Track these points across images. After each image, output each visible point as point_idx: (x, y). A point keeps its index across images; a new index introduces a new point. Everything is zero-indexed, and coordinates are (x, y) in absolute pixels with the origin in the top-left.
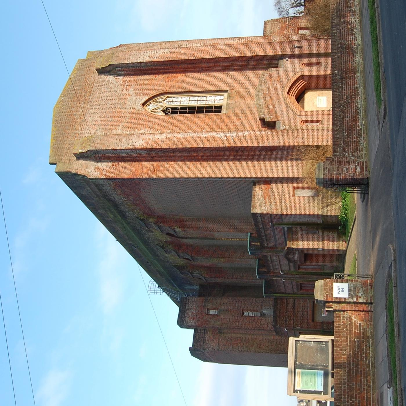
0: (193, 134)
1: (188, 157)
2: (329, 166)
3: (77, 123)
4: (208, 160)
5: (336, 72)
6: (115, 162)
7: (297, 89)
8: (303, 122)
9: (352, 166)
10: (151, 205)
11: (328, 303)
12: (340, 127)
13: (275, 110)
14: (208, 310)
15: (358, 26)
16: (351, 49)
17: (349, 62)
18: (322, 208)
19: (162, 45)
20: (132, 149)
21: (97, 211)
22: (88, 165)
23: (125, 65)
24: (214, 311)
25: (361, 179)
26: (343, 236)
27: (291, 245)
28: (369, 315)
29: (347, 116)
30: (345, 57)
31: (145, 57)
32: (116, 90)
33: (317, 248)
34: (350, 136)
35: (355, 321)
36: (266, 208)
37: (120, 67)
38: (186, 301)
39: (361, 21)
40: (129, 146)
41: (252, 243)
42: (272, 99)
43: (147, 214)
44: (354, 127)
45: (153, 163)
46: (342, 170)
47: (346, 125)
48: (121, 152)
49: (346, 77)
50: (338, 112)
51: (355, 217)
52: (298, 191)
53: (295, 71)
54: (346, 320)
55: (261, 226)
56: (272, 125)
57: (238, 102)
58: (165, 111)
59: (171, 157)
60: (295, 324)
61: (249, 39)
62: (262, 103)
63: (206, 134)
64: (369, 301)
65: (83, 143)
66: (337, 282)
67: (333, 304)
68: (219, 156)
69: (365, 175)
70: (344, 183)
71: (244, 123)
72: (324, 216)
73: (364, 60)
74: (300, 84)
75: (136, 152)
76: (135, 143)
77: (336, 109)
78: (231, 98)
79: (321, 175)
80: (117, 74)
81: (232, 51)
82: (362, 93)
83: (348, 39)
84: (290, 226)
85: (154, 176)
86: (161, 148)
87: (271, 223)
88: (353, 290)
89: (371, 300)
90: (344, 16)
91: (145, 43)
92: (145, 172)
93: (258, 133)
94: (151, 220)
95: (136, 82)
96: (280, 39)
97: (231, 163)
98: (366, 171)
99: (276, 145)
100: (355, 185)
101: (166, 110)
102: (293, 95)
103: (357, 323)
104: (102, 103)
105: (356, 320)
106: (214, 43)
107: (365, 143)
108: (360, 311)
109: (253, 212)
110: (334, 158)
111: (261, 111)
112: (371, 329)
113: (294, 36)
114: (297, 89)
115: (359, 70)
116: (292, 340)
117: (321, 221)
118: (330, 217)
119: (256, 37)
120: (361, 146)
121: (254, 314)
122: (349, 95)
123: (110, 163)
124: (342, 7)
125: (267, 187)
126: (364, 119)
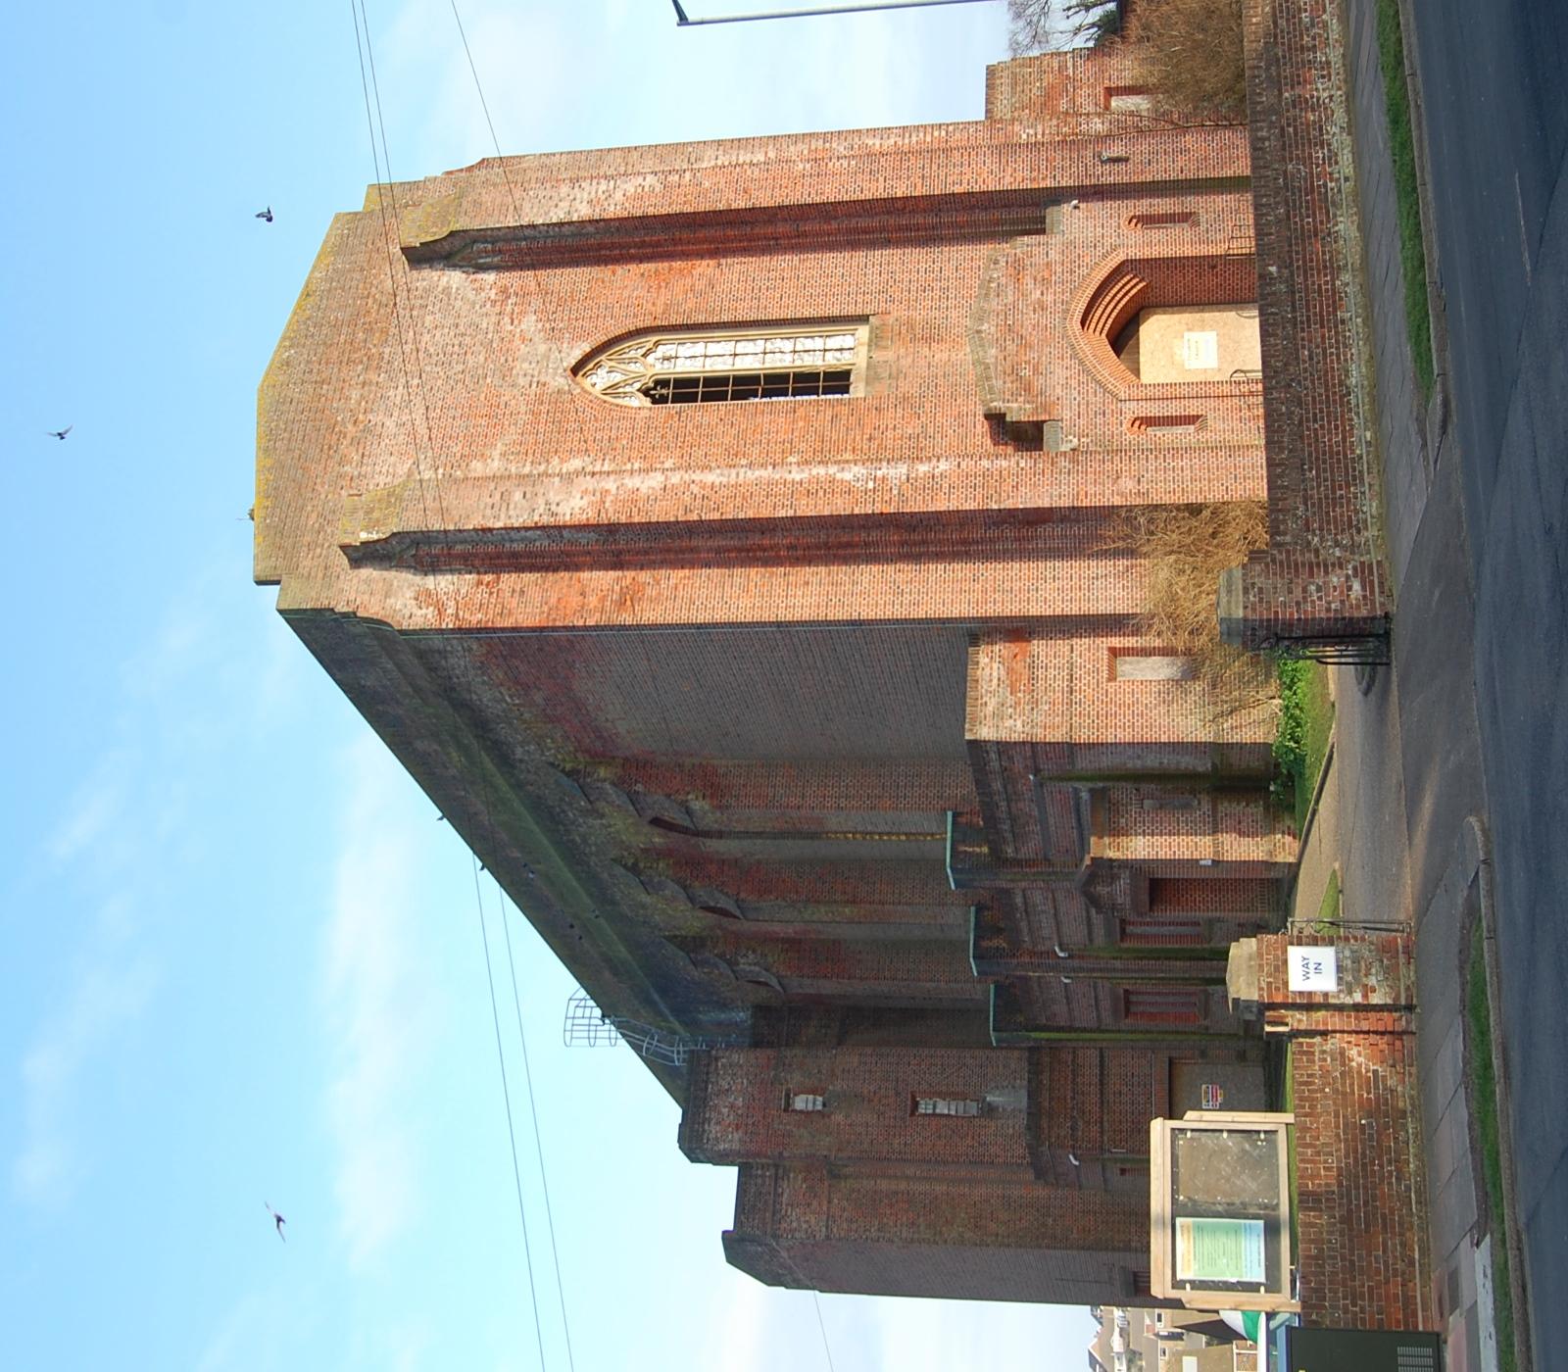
0: (757, 473)
1: (739, 550)
2: (1263, 579)
3: (345, 437)
4: (809, 561)
5: (1273, 269)
6: (486, 573)
7: (1115, 308)
8: (1137, 423)
9: (1335, 579)
10: (607, 720)
11: (1274, 1009)
12: (1290, 451)
13: (1038, 383)
14: (788, 1096)
15: (1340, 115)
16: (1320, 193)
17: (1316, 235)
18: (1211, 718)
19: (631, 161)
20: (548, 526)
21: (410, 743)
22: (392, 585)
23: (506, 234)
24: (811, 1097)
25: (1365, 619)
26: (1287, 817)
27: (1105, 849)
28: (1403, 1046)
29: (1315, 414)
30: (1302, 220)
31: (576, 204)
32: (477, 320)
33: (1197, 861)
34: (1326, 480)
35: (1360, 1065)
36: (1019, 723)
37: (486, 242)
38: (709, 1065)
39: (1350, 98)
40: (536, 518)
41: (962, 848)
42: (1029, 346)
43: (587, 751)
44: (1338, 453)
45: (620, 573)
46: (1305, 590)
47: (1310, 445)
48: (506, 537)
49: (1307, 286)
51: (1333, 747)
52: (1126, 662)
55: (997, 786)
56: (1030, 437)
57: (907, 355)
58: (652, 392)
59: (682, 551)
60: (1106, 1138)
61: (936, 134)
62: (993, 360)
63: (803, 470)
64: (1403, 1002)
65: (372, 510)
67: (1290, 1013)
68: (849, 545)
69: (1377, 605)
70: (1309, 633)
71: (931, 431)
72: (1218, 748)
73: (1364, 228)
74: (1124, 291)
75: (562, 536)
76: (558, 504)
77: (1275, 395)
78: (883, 343)
79: (1237, 608)
80: (477, 264)
81: (881, 179)
82: (1359, 340)
83: (1308, 160)
84: (1101, 785)
85: (626, 618)
86: (650, 523)
87: (1035, 776)
88: (1349, 966)
89: (1409, 997)
90: (1292, 80)
91: (570, 153)
92: (592, 606)
93: (985, 463)
94: (602, 772)
96: (1047, 132)
97: (890, 568)
99: (1047, 505)
100: (1347, 640)
101: (655, 388)
102: (1099, 329)
103: (1367, 1071)
104: (428, 369)
105: (1361, 1059)
106: (813, 147)
107: (1374, 504)
108: (1376, 1032)
109: (972, 738)
110: (1275, 552)
111: (991, 388)
112: (1412, 1089)
113: (1096, 120)
114: (1115, 308)
116: (1159, 1130)
117: (1209, 765)
118: (1241, 748)
119: (961, 127)
120: (1363, 513)
121: (953, 1107)
123: (467, 576)
124: (1284, 51)
125: (1017, 650)
126: (1369, 424)
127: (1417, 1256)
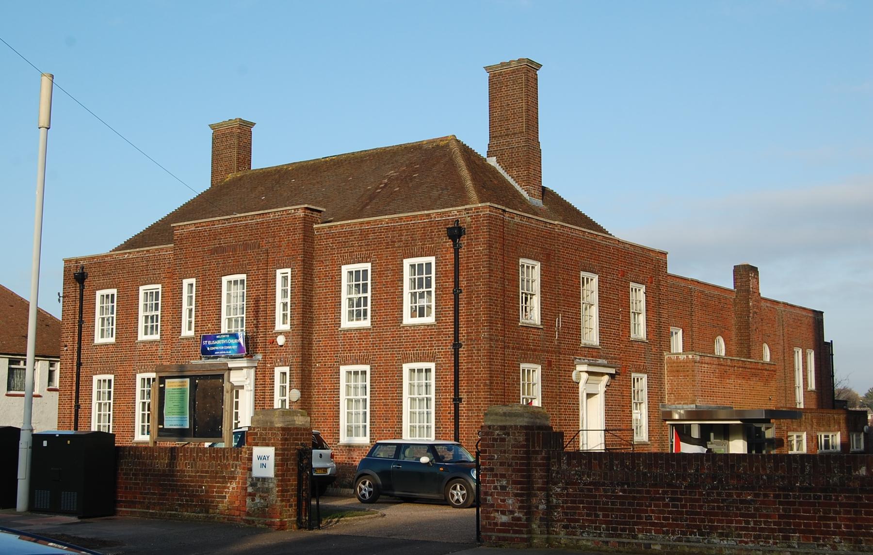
5: (863, 471)
12: (645, 474)
29: (680, 500)
34: (613, 503)
35: (228, 488)
44: (640, 517)
46: (503, 476)
47: (648, 492)
50: (697, 470)
54: (232, 471)
66: (276, 455)
69: (489, 534)
77: (706, 464)
98: (499, 538)
103: (226, 492)
107: (589, 544)
115: (863, 551)
120: (582, 533)
122: (756, 509)
126: (669, 549)
127: (151, 511)
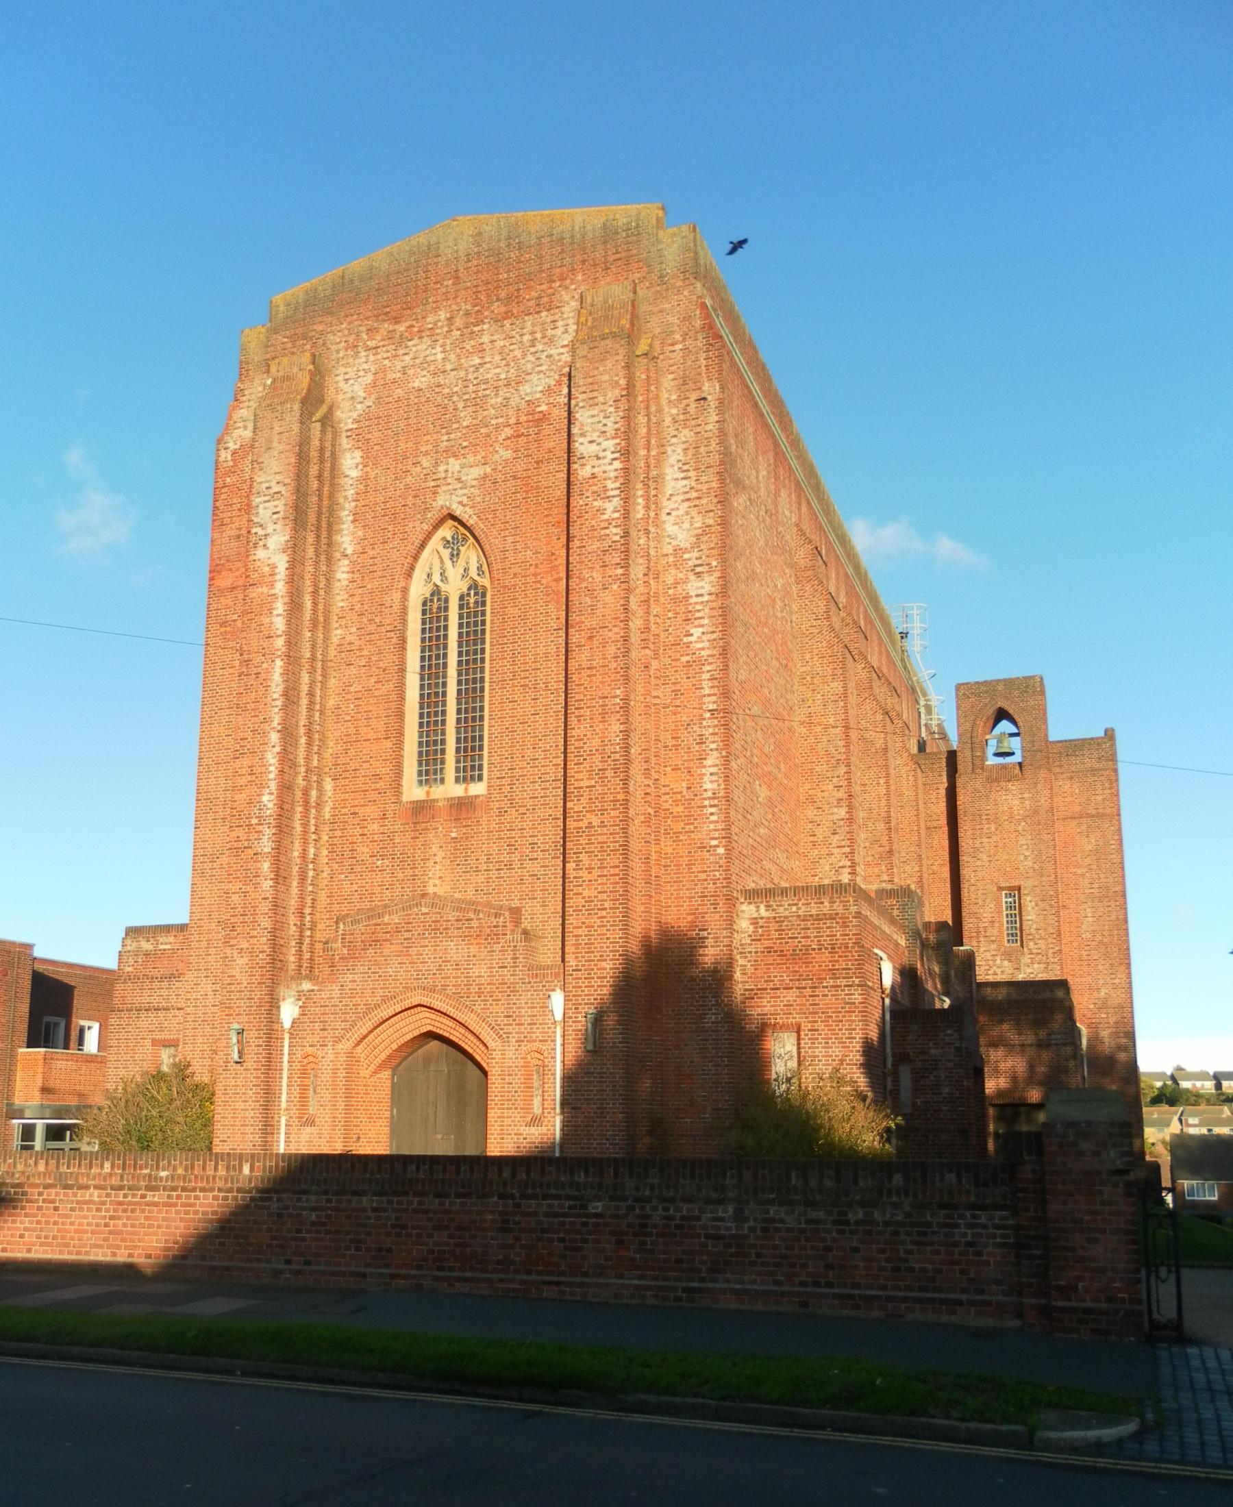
19: (704, 501)
36: (130, 969)
53: (511, 1025)
81: (593, 783)
95: (537, 463)
